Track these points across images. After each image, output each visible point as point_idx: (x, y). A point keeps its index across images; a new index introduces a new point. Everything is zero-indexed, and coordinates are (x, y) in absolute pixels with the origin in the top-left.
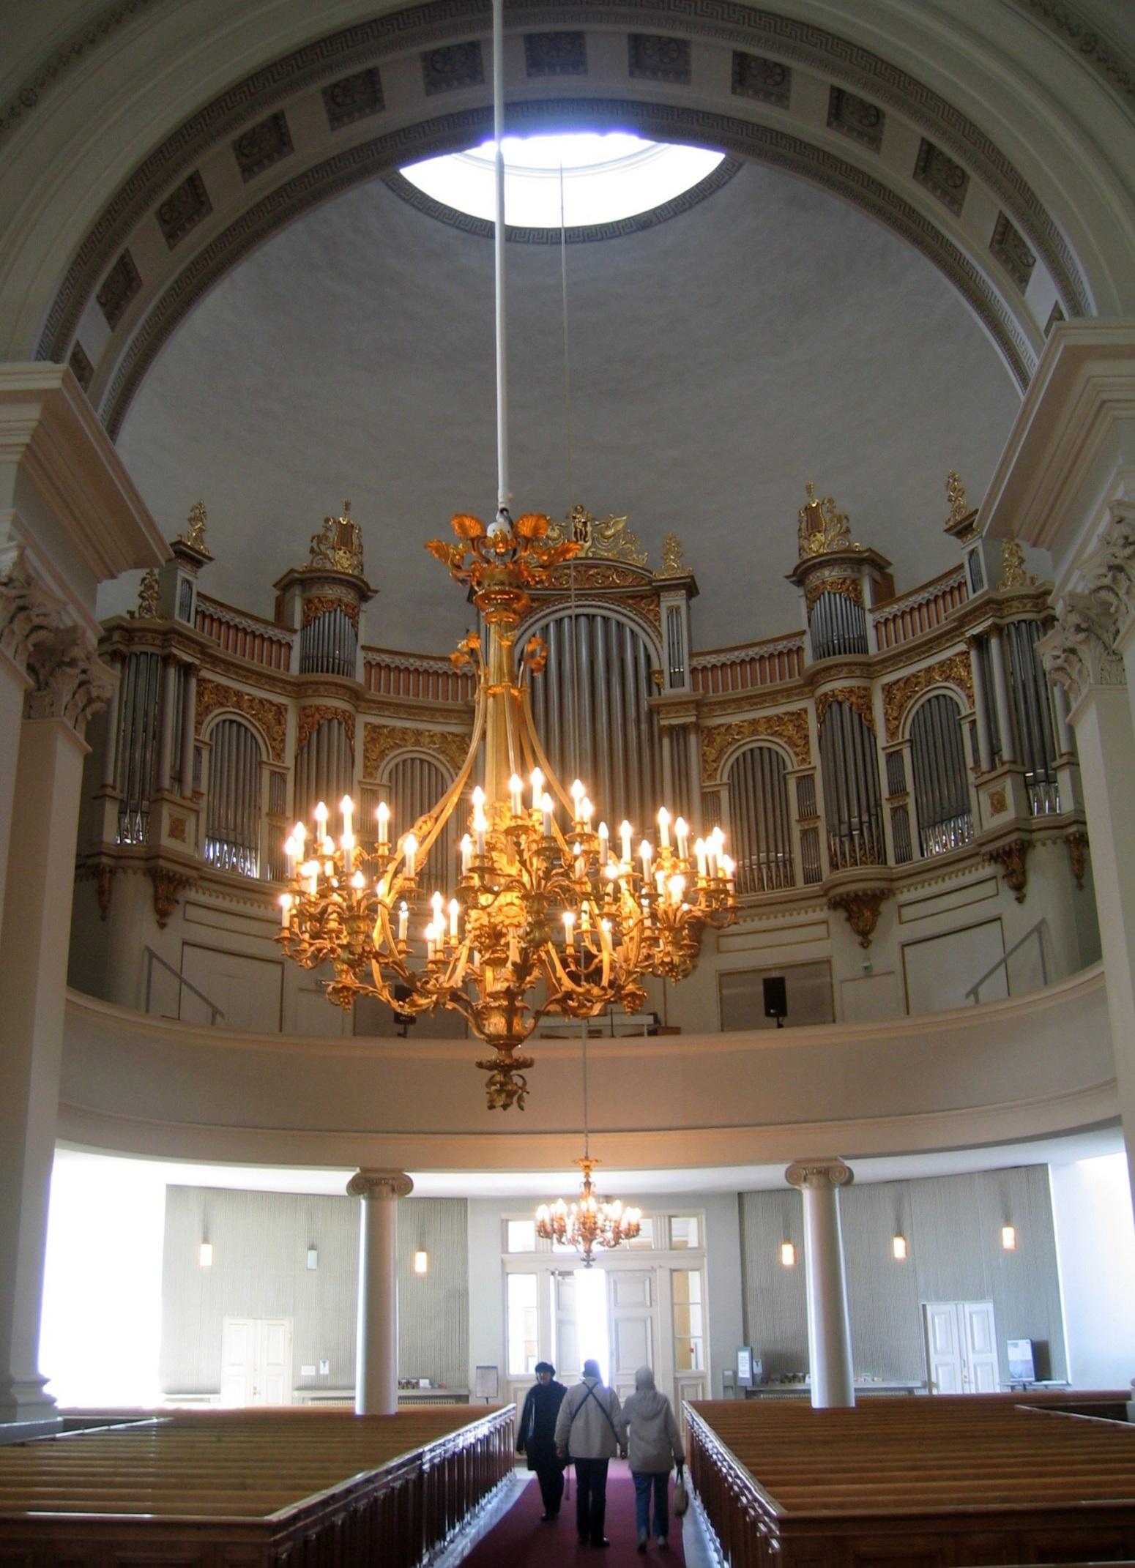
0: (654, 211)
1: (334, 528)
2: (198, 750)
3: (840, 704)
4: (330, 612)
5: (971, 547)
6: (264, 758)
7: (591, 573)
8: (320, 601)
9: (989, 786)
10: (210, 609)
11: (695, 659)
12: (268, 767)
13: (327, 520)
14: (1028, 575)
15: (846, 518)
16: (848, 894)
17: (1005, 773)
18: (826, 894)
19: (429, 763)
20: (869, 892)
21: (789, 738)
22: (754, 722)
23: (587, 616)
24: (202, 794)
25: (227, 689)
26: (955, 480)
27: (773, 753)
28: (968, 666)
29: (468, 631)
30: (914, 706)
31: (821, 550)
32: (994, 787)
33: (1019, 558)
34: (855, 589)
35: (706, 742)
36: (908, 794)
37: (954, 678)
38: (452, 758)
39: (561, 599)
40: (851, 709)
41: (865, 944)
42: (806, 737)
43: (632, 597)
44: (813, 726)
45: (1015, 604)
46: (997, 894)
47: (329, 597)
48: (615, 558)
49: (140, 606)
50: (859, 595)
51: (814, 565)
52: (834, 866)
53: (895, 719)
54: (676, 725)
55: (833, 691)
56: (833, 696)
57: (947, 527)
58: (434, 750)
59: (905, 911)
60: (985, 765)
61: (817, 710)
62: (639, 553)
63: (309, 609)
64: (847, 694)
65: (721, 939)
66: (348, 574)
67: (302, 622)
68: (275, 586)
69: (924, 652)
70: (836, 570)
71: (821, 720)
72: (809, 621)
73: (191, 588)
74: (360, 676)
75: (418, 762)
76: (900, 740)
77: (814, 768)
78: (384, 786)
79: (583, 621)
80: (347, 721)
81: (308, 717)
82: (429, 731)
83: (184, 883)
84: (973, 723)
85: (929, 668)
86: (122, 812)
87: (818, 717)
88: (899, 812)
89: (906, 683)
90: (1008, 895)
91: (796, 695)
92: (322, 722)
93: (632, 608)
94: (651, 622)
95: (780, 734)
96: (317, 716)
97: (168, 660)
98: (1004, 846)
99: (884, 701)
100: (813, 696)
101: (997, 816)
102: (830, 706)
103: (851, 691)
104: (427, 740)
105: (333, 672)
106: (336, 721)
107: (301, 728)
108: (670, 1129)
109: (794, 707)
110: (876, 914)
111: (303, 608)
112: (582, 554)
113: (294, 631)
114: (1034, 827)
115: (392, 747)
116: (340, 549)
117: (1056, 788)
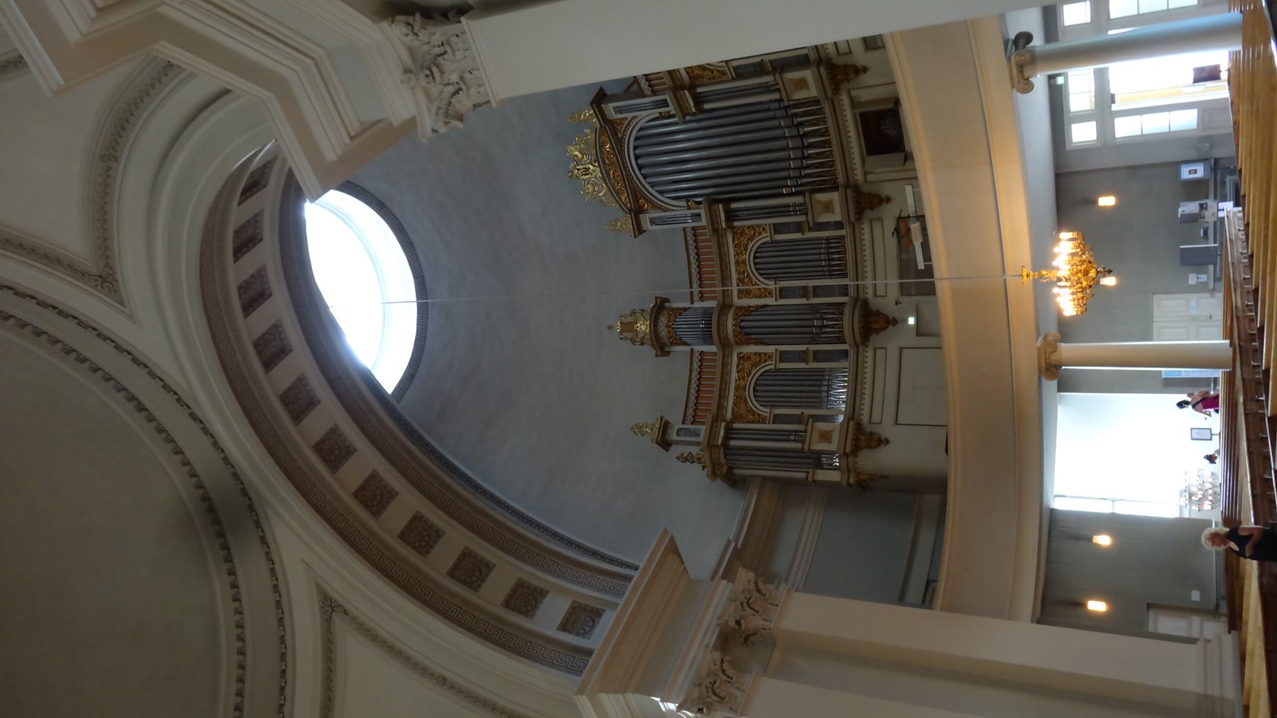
1: (625, 334)
2: (777, 419)
6: (772, 367)
7: (607, 161)
10: (690, 411)
11: (646, 93)
12: (777, 365)
13: (621, 338)
24: (802, 413)
38: (749, 240)
43: (617, 135)
49: (699, 463)
65: (840, 52)
73: (681, 429)
79: (640, 161)
81: (742, 341)
83: (859, 426)
86: (822, 468)
97: (725, 446)
105: (711, 331)
106: (742, 324)
107: (749, 344)
108: (994, 182)
112: (598, 169)
113: (692, 350)
116: (636, 330)
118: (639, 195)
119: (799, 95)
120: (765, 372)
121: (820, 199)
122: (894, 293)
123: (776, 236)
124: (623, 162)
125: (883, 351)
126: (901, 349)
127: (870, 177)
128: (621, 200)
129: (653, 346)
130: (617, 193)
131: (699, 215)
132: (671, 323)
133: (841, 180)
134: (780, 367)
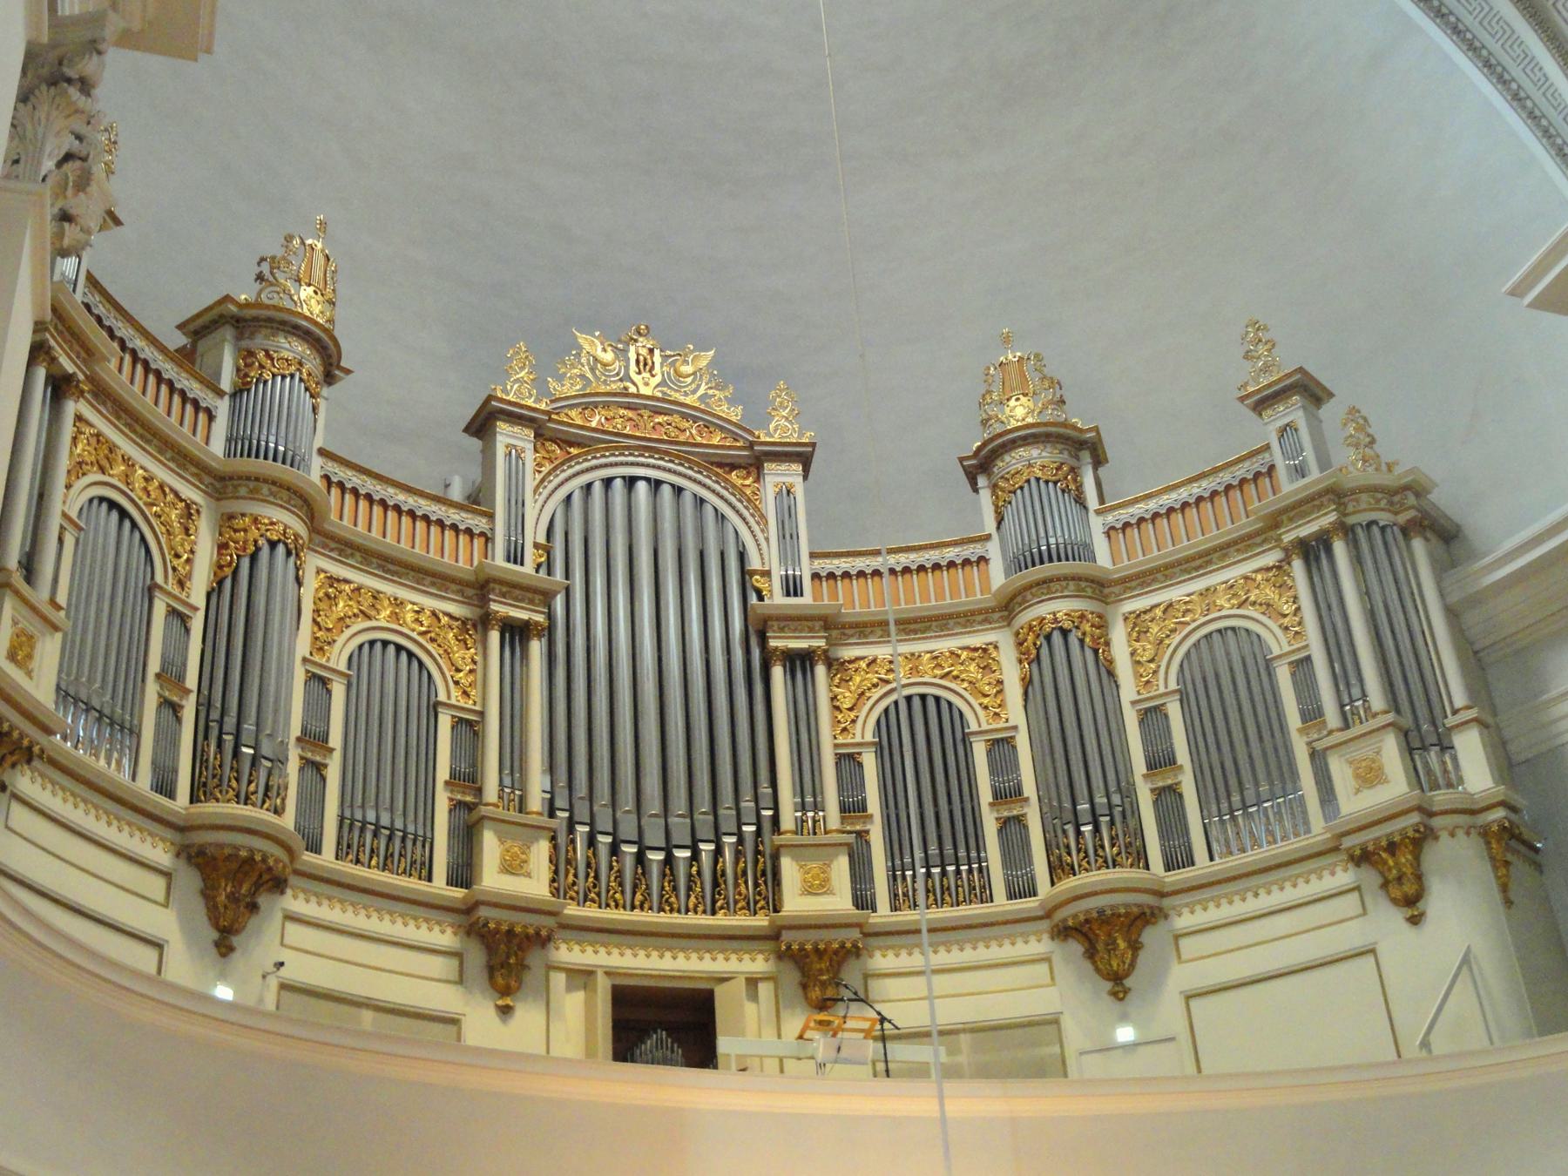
3: (1065, 633)
4: (284, 377)
5: (1286, 421)
6: (159, 579)
8: (268, 355)
9: (1352, 746)
13: (289, 238)
15: (1059, 383)
16: (1101, 912)
17: (1384, 727)
19: (411, 655)
21: (970, 682)
22: (913, 657)
23: (648, 480)
25: (112, 448)
27: (944, 706)
30: (1179, 646)
31: (1030, 420)
32: (1363, 751)
33: (1369, 435)
34: (1075, 480)
35: (837, 680)
36: (1181, 767)
37: (1254, 604)
39: (616, 448)
40: (1082, 641)
42: (1000, 682)
43: (720, 465)
45: (1364, 497)
47: (285, 354)
48: (697, 405)
50: (1080, 488)
51: (1013, 441)
53: (1151, 661)
54: (792, 649)
55: (1054, 614)
56: (1056, 620)
58: (422, 634)
59: (1184, 942)
62: (731, 401)
63: (246, 365)
66: (316, 323)
67: (234, 384)
68: (180, 327)
71: (1030, 658)
75: (391, 649)
76: (1162, 690)
77: (1015, 728)
81: (236, 531)
82: (414, 604)
84: (1302, 666)
85: (1207, 590)
88: (1168, 797)
89: (1164, 612)
90: (1394, 918)
91: (980, 623)
94: (749, 500)
95: (956, 677)
96: (254, 533)
99: (1130, 634)
100: (1009, 625)
101: (1366, 793)
102: (1048, 638)
103: (1082, 617)
104: (409, 617)
107: (222, 547)
110: (1135, 947)
113: (220, 393)
114: (1435, 809)
117: (1455, 759)
118: (574, 451)
120: (148, 551)
124: (657, 451)
125: (161, 897)
126: (158, 945)
127: (558, 980)
128: (571, 407)
129: (248, 305)
130: (586, 407)
132: (305, 376)
133: (572, 910)
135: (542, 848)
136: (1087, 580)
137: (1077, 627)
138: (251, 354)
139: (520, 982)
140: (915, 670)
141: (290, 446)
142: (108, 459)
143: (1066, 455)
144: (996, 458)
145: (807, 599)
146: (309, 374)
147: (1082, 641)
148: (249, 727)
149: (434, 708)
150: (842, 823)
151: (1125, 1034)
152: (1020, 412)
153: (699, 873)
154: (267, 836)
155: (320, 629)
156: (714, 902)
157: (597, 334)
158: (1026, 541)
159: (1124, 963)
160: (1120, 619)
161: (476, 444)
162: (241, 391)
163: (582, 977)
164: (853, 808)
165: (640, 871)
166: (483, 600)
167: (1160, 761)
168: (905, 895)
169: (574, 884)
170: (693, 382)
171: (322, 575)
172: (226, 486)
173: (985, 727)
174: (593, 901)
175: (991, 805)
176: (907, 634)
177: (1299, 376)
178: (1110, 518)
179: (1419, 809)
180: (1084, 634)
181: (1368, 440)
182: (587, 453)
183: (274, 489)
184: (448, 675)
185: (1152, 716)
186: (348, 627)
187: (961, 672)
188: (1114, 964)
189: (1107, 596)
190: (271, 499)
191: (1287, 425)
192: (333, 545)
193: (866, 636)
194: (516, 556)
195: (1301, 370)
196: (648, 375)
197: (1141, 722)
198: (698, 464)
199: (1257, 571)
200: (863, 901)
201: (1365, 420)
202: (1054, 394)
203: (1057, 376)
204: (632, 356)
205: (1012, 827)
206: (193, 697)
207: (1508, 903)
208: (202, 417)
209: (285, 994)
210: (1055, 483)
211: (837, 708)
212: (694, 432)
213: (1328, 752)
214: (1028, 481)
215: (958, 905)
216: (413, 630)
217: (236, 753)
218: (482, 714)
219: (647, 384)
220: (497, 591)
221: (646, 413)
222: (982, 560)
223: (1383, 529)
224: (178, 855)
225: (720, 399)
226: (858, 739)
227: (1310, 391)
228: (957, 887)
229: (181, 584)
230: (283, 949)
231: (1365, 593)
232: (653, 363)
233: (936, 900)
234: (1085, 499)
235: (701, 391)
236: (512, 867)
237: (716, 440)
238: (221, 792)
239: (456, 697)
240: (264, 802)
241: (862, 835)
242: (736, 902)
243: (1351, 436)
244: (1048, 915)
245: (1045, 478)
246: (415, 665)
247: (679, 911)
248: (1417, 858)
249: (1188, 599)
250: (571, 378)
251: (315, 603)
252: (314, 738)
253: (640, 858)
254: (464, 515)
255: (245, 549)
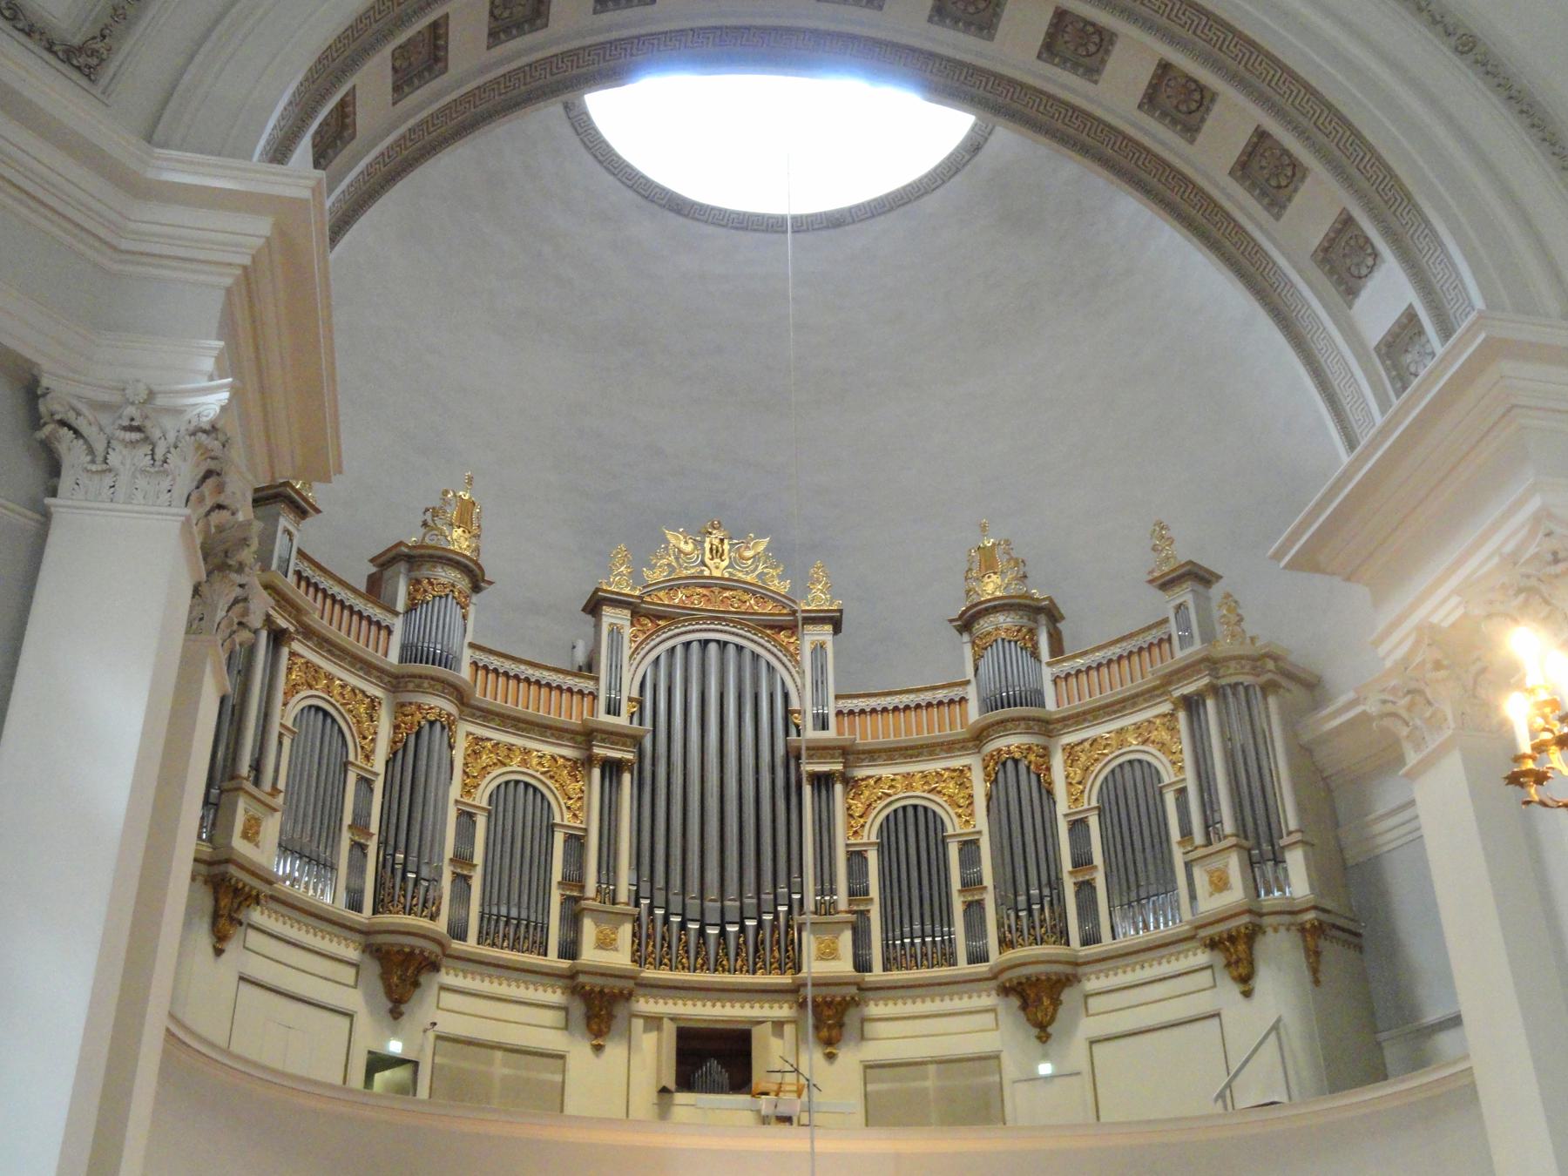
0: (850, 210)
3: (1016, 762)
5: (1178, 602)
6: (351, 757)
8: (431, 583)
9: (1208, 861)
13: (446, 492)
14: (1248, 634)
15: (1023, 561)
16: (1028, 978)
17: (1231, 847)
18: (995, 977)
19: (535, 789)
20: (1054, 978)
21: (949, 796)
22: (907, 776)
23: (718, 642)
25: (317, 669)
26: (1162, 528)
27: (930, 814)
28: (1172, 729)
29: (574, 647)
30: (1100, 772)
31: (998, 594)
32: (1217, 863)
33: (1238, 615)
36: (1096, 867)
37: (1153, 742)
39: (693, 619)
40: (1028, 768)
41: (1044, 1036)
42: (971, 796)
43: (771, 627)
44: (979, 789)
46: (1215, 986)
47: (442, 580)
48: (754, 581)
50: (1035, 646)
51: (986, 609)
52: (1005, 944)
53: (1080, 783)
55: (1008, 747)
56: (1009, 752)
57: (1150, 577)
58: (543, 773)
59: (1091, 1001)
60: (1199, 838)
61: (985, 768)
62: (782, 578)
64: (1025, 752)
66: (465, 556)
67: (406, 605)
68: (372, 561)
69: (1115, 712)
70: (1012, 616)
72: (976, 670)
73: (291, 540)
74: (465, 672)
75: (522, 786)
76: (1086, 806)
77: (979, 832)
78: (483, 809)
79: (713, 647)
80: (448, 726)
81: (406, 715)
82: (538, 751)
84: (1182, 792)
85: (1122, 729)
87: (988, 775)
88: (1085, 889)
89: (1091, 745)
90: (1231, 991)
91: (959, 750)
92: (423, 723)
93: (770, 639)
94: (792, 655)
95: (939, 792)
96: (418, 716)
98: (1229, 930)
99: (1065, 762)
100: (979, 752)
102: (1004, 764)
103: (1029, 749)
104: (535, 761)
106: (438, 725)
107: (396, 727)
109: (957, 763)
110: (1056, 1002)
111: (408, 588)
112: (717, 573)
113: (396, 614)
114: (1265, 910)
115: (495, 764)
116: (459, 527)
117: (1285, 870)
118: (662, 623)
119: (810, 943)
121: (621, 929)
122: (451, 1025)
123: (562, 835)
124: (724, 619)
125: (351, 981)
126: (349, 1015)
127: (638, 1024)
131: (617, 713)
133: (649, 973)
134: (349, 772)
135: (626, 930)
136: (1034, 720)
137: (1026, 757)
138: (418, 582)
139: (609, 1028)
140: (909, 787)
141: (445, 649)
142: (314, 677)
143: (1025, 620)
144: (974, 622)
145: (831, 734)
146: (460, 592)
147: (1028, 768)
148: (413, 859)
149: (551, 828)
150: (850, 905)
151: (1045, 1069)
152: (990, 588)
153: (745, 942)
154: (424, 937)
155: (468, 777)
156: (755, 963)
157: (681, 530)
158: (998, 686)
159: (1046, 1015)
160: (1060, 751)
161: (589, 617)
162: (411, 610)
163: (654, 1022)
164: (858, 891)
165: (701, 941)
166: (590, 747)
167: (1082, 861)
168: (895, 959)
169: (652, 952)
170: (752, 563)
171: (471, 737)
172: (399, 683)
173: (959, 831)
174: (666, 965)
175: (960, 891)
176: (905, 758)
177: (1188, 568)
178: (1055, 670)
179: (1250, 911)
180: (1030, 762)
181: (1238, 618)
182: (669, 625)
183: (432, 683)
184: (562, 802)
185: (1078, 827)
186: (489, 773)
187: (943, 788)
188: (1039, 1015)
189: (1051, 731)
190: (430, 690)
191: (1181, 604)
192: (479, 713)
193: (874, 760)
194: (613, 708)
195: (1190, 562)
196: (718, 560)
197: (1070, 831)
198: (754, 629)
199: (1157, 717)
200: (862, 965)
201: (1236, 602)
202: (1018, 571)
203: (1021, 557)
204: (707, 546)
205: (974, 910)
206: (375, 838)
207: (1317, 982)
208: (383, 633)
209: (440, 1043)
210: (1016, 642)
211: (851, 816)
212: (752, 602)
213: (1194, 863)
214: (996, 641)
215: (933, 967)
216: (537, 771)
217: (404, 878)
218: (586, 830)
219: (717, 568)
220: (599, 738)
221: (716, 590)
222: (963, 700)
223: (1247, 688)
224: (364, 951)
225: (773, 576)
226: (865, 840)
227: (1200, 576)
228: (933, 953)
229: (367, 758)
230: (440, 1012)
231: (1226, 739)
232: (723, 550)
233: (916, 962)
234: (1039, 653)
235: (760, 568)
236: (604, 944)
237: (769, 608)
238: (393, 906)
239: (568, 818)
240: (423, 911)
241: (864, 914)
242: (771, 964)
243: (1224, 616)
244: (995, 977)
245: (1008, 638)
246: (539, 797)
247: (729, 971)
248: (1250, 948)
249: (1108, 735)
250: (660, 567)
251: (465, 759)
252: (462, 859)
253: (702, 932)
254: (577, 680)
255: (411, 729)
